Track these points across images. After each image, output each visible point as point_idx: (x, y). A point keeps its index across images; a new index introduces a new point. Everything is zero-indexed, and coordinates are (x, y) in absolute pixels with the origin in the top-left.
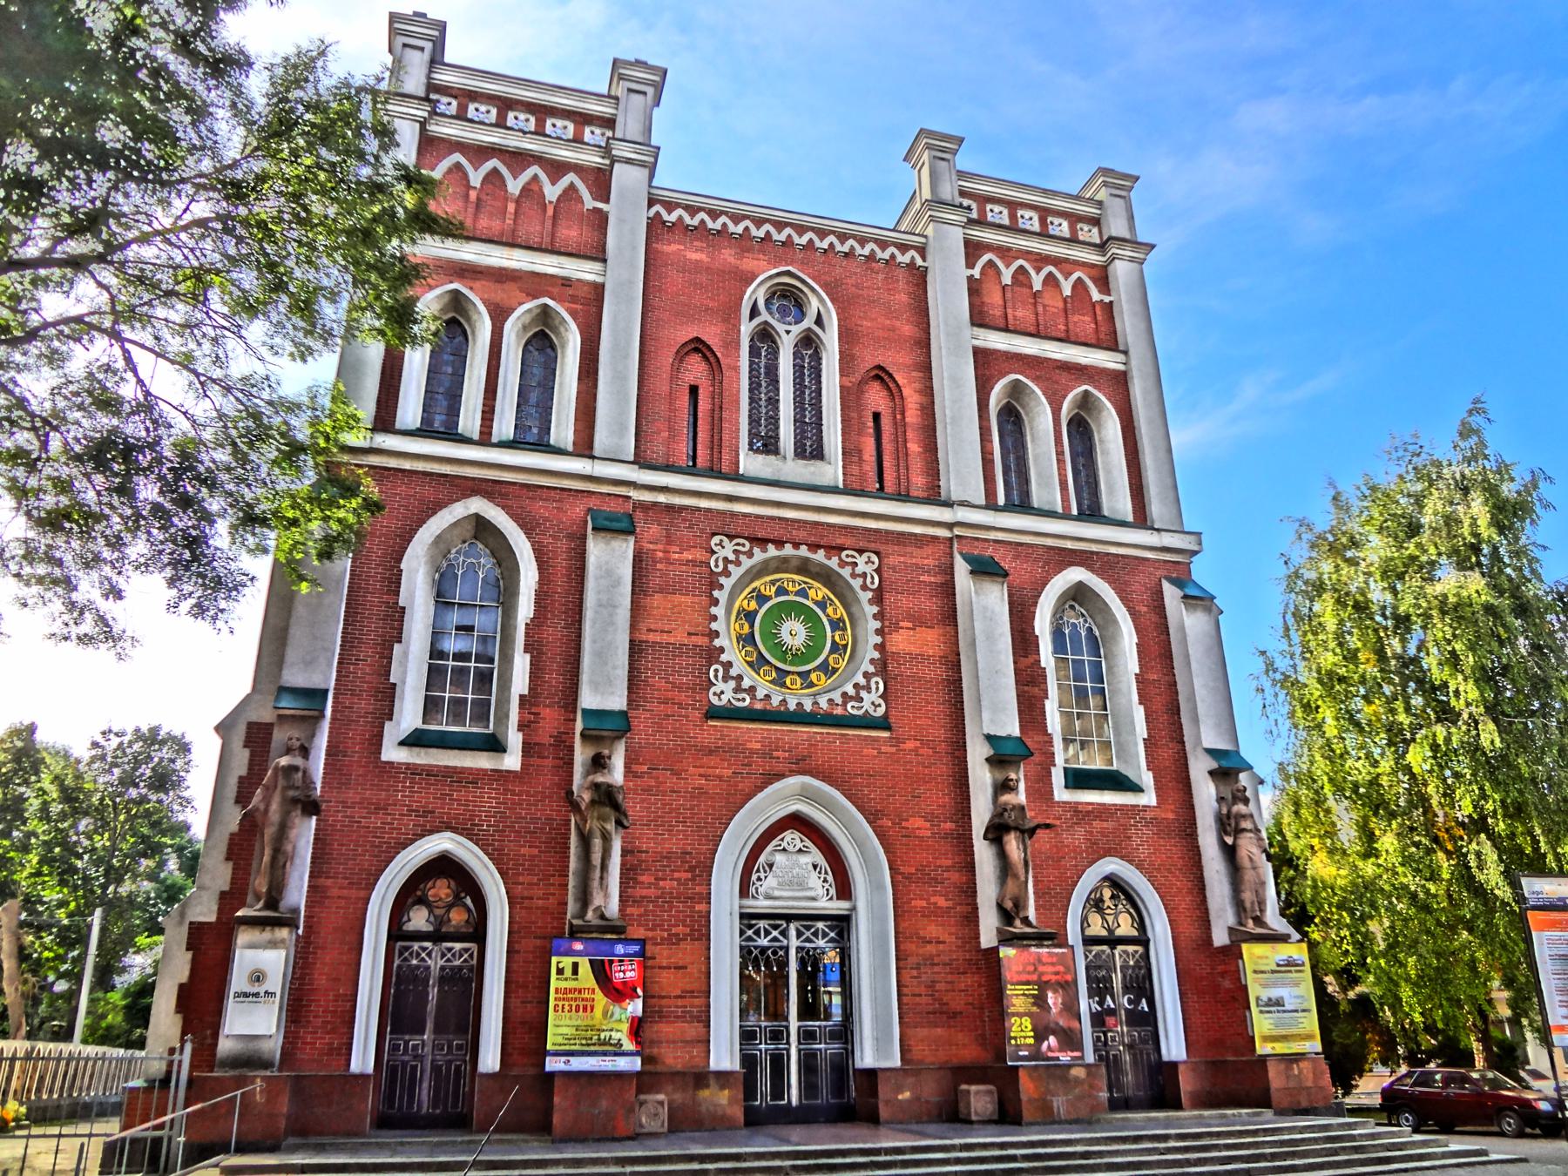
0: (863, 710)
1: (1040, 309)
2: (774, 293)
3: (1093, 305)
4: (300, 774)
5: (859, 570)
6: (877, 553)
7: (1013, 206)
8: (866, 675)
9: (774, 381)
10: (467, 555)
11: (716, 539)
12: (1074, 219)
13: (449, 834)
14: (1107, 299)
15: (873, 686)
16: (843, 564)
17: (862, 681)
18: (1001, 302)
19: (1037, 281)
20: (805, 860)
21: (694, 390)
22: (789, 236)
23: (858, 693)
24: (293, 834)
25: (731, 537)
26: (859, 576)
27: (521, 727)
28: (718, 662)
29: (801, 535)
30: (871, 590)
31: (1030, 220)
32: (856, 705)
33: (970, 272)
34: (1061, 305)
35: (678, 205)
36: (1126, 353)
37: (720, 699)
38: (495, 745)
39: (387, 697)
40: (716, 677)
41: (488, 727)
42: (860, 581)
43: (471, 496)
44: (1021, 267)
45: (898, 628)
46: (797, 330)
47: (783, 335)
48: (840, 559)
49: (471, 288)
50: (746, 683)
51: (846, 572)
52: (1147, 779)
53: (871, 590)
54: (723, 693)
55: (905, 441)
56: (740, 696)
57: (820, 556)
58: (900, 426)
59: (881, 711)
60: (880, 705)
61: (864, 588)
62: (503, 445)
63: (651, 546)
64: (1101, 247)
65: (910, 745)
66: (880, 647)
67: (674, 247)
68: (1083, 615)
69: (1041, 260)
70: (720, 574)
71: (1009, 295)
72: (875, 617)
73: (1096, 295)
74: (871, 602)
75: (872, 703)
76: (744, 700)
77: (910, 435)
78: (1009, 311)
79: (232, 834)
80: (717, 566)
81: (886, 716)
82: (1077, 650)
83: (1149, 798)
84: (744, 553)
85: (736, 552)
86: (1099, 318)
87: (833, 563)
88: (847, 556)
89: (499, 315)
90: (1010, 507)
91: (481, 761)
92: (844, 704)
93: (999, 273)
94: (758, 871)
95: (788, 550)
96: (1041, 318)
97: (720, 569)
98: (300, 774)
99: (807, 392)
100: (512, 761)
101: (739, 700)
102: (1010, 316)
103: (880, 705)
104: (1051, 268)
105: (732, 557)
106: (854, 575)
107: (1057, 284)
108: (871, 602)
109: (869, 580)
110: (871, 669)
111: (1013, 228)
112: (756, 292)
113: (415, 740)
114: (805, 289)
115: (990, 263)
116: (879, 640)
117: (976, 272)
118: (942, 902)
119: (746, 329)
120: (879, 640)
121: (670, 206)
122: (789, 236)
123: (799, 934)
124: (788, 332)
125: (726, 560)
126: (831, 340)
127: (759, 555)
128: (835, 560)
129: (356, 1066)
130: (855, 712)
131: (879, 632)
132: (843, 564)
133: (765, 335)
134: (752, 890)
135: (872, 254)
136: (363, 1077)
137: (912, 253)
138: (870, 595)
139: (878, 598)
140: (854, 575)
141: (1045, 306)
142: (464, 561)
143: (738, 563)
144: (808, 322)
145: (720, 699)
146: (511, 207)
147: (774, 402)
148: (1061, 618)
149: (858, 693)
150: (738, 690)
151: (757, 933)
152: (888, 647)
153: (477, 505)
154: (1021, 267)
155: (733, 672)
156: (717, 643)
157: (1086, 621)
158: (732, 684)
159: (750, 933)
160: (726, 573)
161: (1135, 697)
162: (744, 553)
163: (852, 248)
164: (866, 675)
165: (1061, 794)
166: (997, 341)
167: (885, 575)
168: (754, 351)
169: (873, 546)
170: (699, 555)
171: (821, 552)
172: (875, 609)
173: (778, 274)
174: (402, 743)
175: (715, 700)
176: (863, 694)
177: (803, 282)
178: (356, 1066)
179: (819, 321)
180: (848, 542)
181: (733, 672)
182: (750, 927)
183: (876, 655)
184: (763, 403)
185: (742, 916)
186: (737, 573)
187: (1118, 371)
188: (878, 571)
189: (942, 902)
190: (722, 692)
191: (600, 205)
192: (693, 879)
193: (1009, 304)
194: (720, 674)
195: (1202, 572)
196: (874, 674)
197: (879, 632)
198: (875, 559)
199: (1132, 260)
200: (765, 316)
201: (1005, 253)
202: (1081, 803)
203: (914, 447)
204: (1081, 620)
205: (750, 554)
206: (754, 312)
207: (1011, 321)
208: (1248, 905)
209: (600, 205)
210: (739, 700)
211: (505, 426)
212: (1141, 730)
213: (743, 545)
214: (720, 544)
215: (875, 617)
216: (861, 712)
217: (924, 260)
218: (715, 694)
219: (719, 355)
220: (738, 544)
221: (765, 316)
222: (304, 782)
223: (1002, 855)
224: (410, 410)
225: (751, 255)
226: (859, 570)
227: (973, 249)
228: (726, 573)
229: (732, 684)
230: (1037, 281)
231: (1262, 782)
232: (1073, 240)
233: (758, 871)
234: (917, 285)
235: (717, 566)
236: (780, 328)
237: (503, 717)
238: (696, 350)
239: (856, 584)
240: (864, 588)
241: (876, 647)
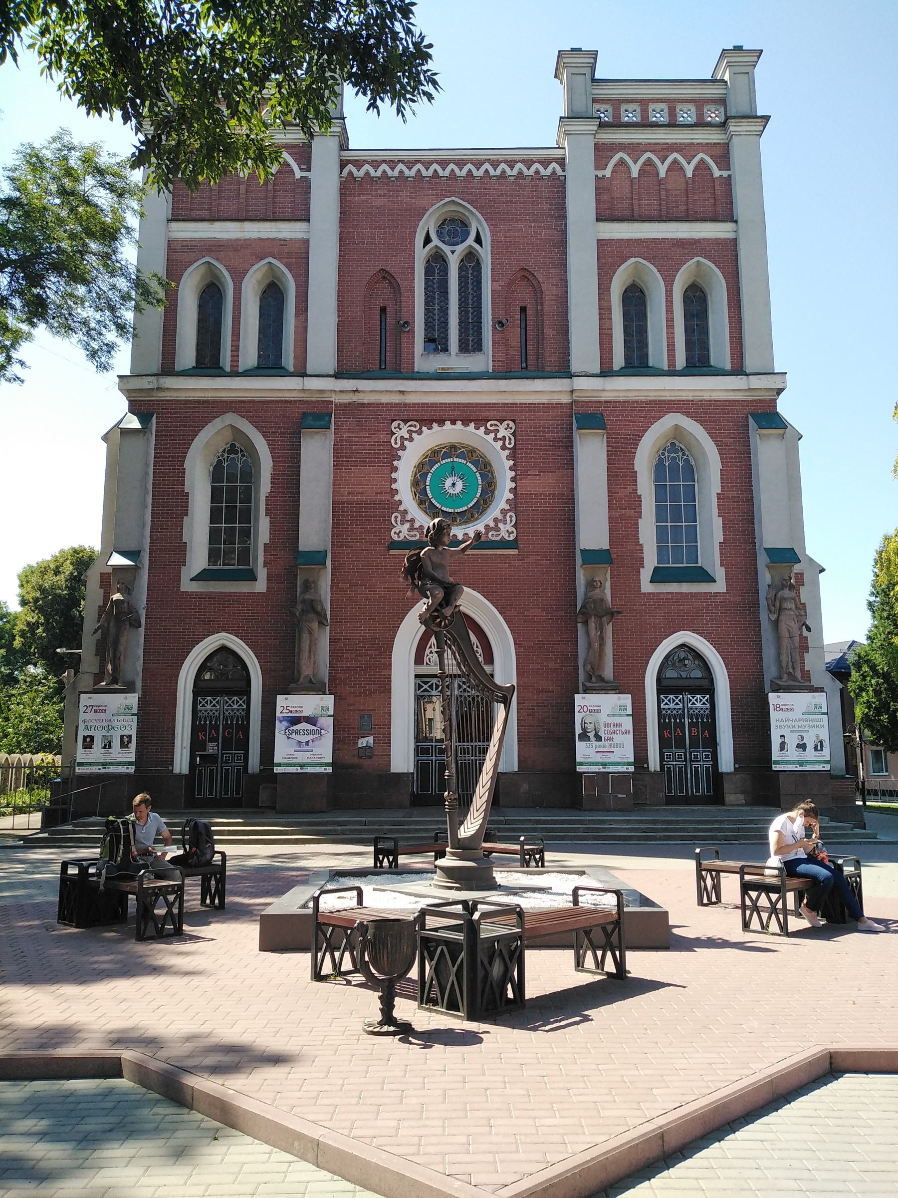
0: (500, 537)
1: (663, 194)
2: (445, 220)
3: (713, 180)
4: (126, 605)
5: (499, 435)
6: (514, 421)
7: (644, 103)
8: (504, 512)
9: (445, 293)
10: (229, 452)
11: (395, 424)
12: (701, 103)
13: (224, 634)
14: (725, 174)
15: (508, 519)
16: (487, 432)
17: (500, 517)
18: (629, 195)
19: (662, 170)
21: (383, 310)
22: (452, 170)
23: (496, 525)
24: (123, 640)
25: (406, 422)
26: (500, 439)
27: (266, 564)
28: (397, 511)
29: (457, 413)
30: (509, 449)
31: (658, 114)
32: (495, 533)
33: (600, 174)
34: (683, 186)
35: (365, 162)
36: (736, 222)
37: (399, 537)
38: (251, 576)
39: (180, 550)
40: (396, 521)
41: (249, 565)
42: (500, 443)
43: (224, 413)
44: (649, 159)
45: (527, 475)
46: (460, 249)
47: (449, 254)
48: (486, 428)
49: (217, 259)
50: (416, 525)
52: (719, 573)
53: (509, 449)
54: (400, 532)
55: (543, 328)
56: (412, 533)
58: (539, 314)
59: (512, 538)
60: (512, 532)
61: (504, 448)
62: (248, 374)
63: (349, 434)
64: (723, 125)
65: (532, 559)
66: (514, 491)
67: (363, 197)
68: (682, 450)
69: (664, 150)
70: (398, 449)
71: (636, 186)
72: (511, 469)
73: (717, 173)
74: (508, 458)
75: (507, 531)
76: (415, 536)
77: (546, 323)
78: (635, 201)
79: (97, 640)
80: (396, 443)
81: (516, 539)
82: (674, 477)
83: (720, 586)
84: (415, 432)
85: (410, 432)
86: (718, 192)
88: (491, 425)
89: (239, 277)
91: (243, 587)
92: (487, 533)
93: (629, 169)
94: (430, 647)
96: (664, 206)
97: (398, 445)
98: (126, 605)
99: (470, 297)
100: (261, 585)
101: (412, 536)
102: (636, 206)
103: (512, 532)
104: (675, 155)
105: (407, 436)
106: (496, 439)
107: (682, 169)
108: (508, 458)
109: (507, 441)
110: (507, 507)
111: (645, 124)
112: (429, 223)
113: (203, 576)
114: (467, 214)
115: (622, 162)
116: (513, 485)
117: (608, 173)
118: (552, 665)
119: (421, 254)
120: (513, 485)
121: (358, 164)
122: (452, 170)
123: (460, 687)
124: (453, 252)
125: (402, 436)
126: (485, 254)
128: (482, 429)
129: (177, 770)
130: (493, 539)
131: (513, 479)
132: (487, 432)
134: (426, 659)
135: (520, 173)
136: (180, 776)
137: (554, 165)
138: (507, 452)
139: (513, 456)
140: (496, 439)
141: (666, 190)
142: (228, 457)
144: (470, 241)
145: (399, 537)
146: (243, 188)
147: (445, 311)
148: (663, 454)
149: (496, 525)
150: (411, 529)
151: (431, 687)
152: (518, 490)
153: (230, 419)
154: (649, 159)
155: (408, 517)
156: (397, 498)
157: (684, 454)
158: (407, 525)
159: (426, 687)
161: (715, 511)
162: (415, 432)
163: (504, 171)
165: (647, 587)
167: (518, 436)
168: (429, 271)
169: (510, 416)
170: (383, 437)
171: (472, 425)
172: (511, 463)
173: (444, 204)
174: (192, 580)
175: (395, 538)
176: (500, 525)
177: (464, 207)
178: (177, 770)
179: (478, 240)
180: (491, 415)
181: (408, 517)
182: (426, 683)
183: (511, 496)
184: (436, 312)
185: (417, 676)
187: (726, 241)
188: (514, 434)
189: (552, 665)
190: (400, 532)
191: (305, 174)
192: (380, 654)
193: (636, 196)
194: (399, 519)
195: (783, 407)
196: (509, 511)
197: (513, 479)
198: (512, 424)
199: (749, 134)
200: (435, 241)
201: (634, 150)
202: (664, 593)
203: (549, 332)
204: (680, 454)
205: (420, 432)
206: (427, 240)
207: (636, 210)
208: (784, 664)
209: (305, 174)
210: (412, 536)
211: (250, 356)
212: (718, 536)
213: (415, 426)
214: (398, 427)
215: (511, 469)
216: (498, 538)
217: (564, 170)
218: (395, 533)
219: (399, 280)
220: (411, 426)
221: (435, 241)
222: (128, 609)
223: (588, 633)
224: (187, 355)
225: (422, 193)
226: (499, 435)
227: (602, 152)
228: (403, 448)
229: (407, 525)
230: (662, 170)
231: (822, 570)
232: (700, 124)
233: (430, 647)
234: (558, 192)
235: (396, 443)
236: (446, 249)
237: (256, 558)
238: (384, 278)
240: (504, 448)
241: (511, 490)
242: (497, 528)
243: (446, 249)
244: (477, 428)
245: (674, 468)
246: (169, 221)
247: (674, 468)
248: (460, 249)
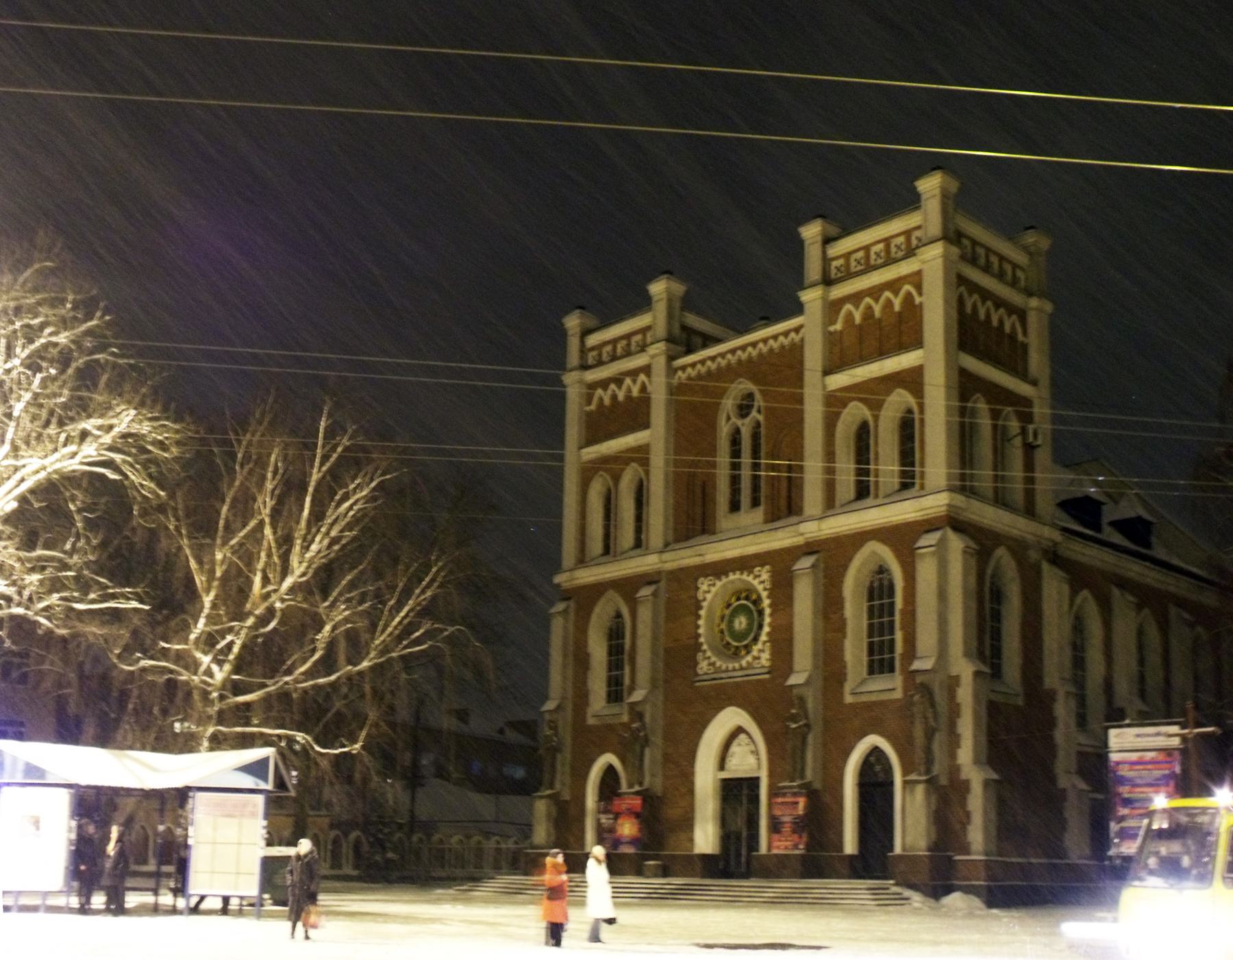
20: (747, 749)
28: (701, 651)
51: (755, 582)
57: (745, 577)
87: (750, 578)
90: (847, 508)
95: (732, 577)
112: (729, 404)
119: (724, 430)
121: (683, 368)
127: (719, 584)
133: (737, 431)
143: (709, 592)
144: (754, 413)
150: (710, 664)
160: (705, 599)
164: (765, 642)
165: (849, 699)
166: (839, 380)
171: (746, 573)
186: (709, 596)
200: (734, 419)
206: (729, 418)
221: (734, 419)
236: (739, 422)
239: (760, 588)
242: (758, 658)
243: (739, 422)
244: (748, 575)
245: (881, 585)
246: (581, 448)
247: (881, 585)
248: (747, 420)
